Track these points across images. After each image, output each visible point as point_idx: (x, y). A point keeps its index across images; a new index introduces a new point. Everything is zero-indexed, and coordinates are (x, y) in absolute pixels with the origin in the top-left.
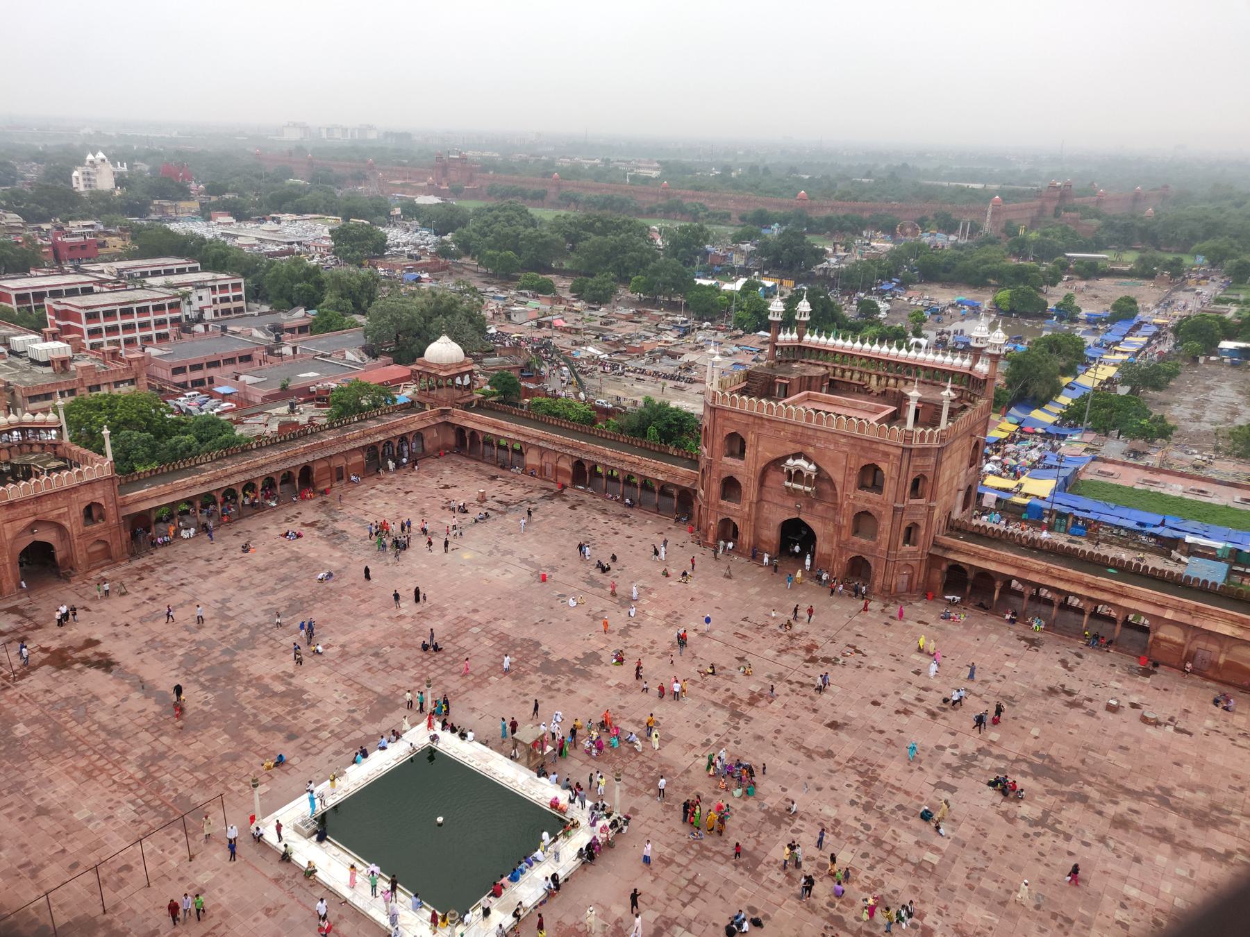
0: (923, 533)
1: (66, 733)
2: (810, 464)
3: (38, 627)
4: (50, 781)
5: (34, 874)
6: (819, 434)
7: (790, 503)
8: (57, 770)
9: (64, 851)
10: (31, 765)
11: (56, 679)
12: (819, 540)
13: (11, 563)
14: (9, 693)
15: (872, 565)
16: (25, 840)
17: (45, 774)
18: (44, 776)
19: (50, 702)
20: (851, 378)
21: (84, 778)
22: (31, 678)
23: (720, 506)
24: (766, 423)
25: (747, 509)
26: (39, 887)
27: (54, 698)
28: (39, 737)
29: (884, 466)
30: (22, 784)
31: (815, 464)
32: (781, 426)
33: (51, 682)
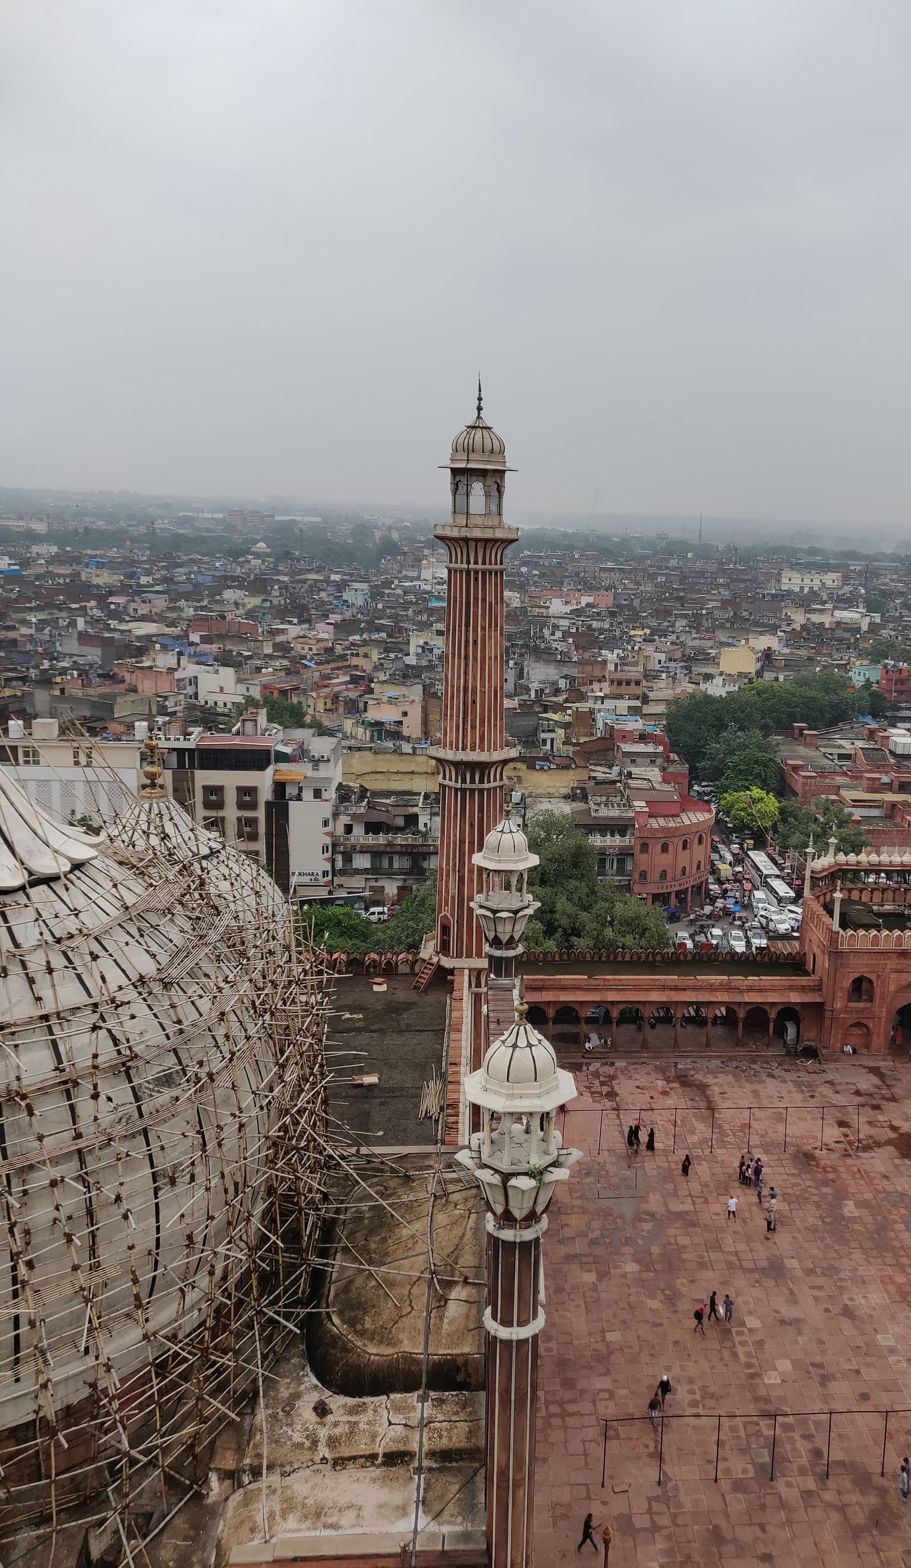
1: (892, 1234)
3: (894, 1099)
4: (864, 1283)
5: (825, 1380)
8: (873, 1272)
9: (858, 1372)
10: (851, 1253)
11: (896, 1166)
13: (886, 1018)
14: (849, 1161)
16: (824, 1336)
17: (861, 1271)
18: (859, 1274)
19: (885, 1191)
21: (898, 1298)
22: (874, 1154)
26: (825, 1399)
27: (890, 1188)
28: (864, 1225)
30: (837, 1270)
33: (891, 1169)
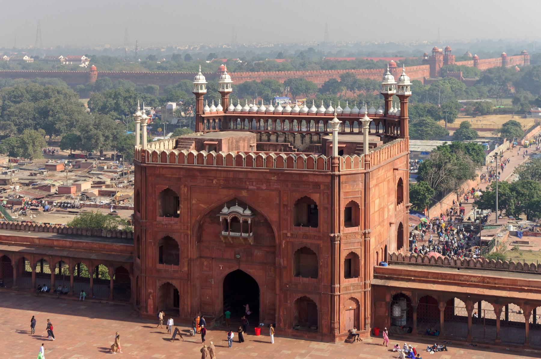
0: (362, 262)
2: (245, 209)
7: (229, 254)
12: (263, 289)
15: (318, 304)
20: (277, 141)
23: (159, 271)
25: (186, 269)
29: (316, 197)
31: (251, 209)
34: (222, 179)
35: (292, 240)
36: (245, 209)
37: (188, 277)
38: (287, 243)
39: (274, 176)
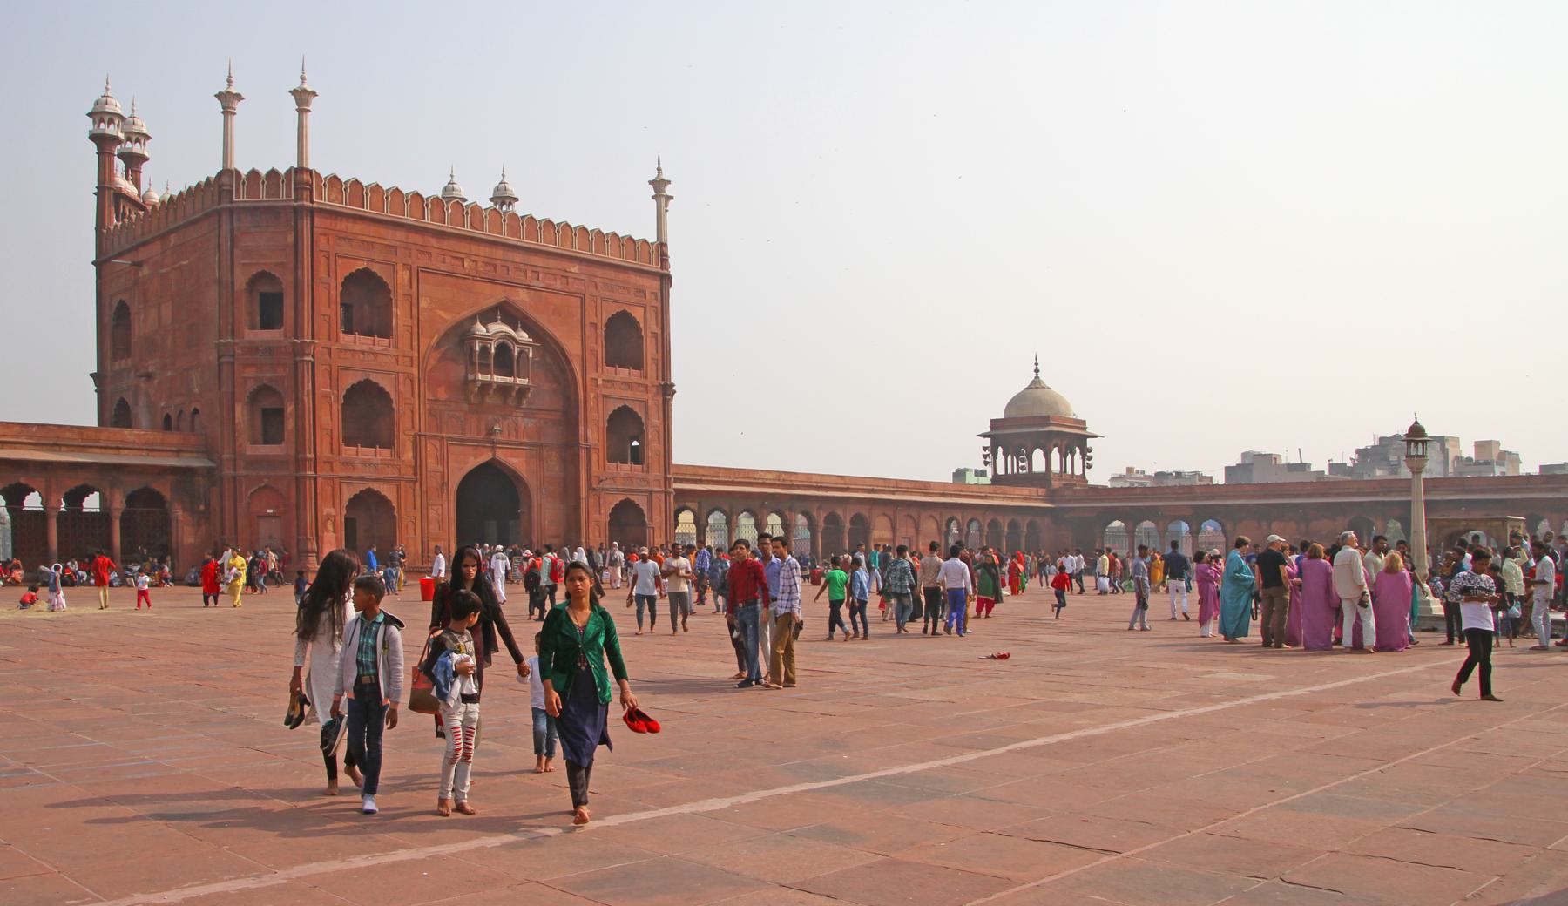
6: (536, 260)
23: (348, 464)
24: (433, 241)
29: (638, 313)
32: (464, 247)
34: (482, 259)
35: (604, 391)
36: (515, 329)
37: (415, 474)
38: (597, 397)
39: (574, 267)
